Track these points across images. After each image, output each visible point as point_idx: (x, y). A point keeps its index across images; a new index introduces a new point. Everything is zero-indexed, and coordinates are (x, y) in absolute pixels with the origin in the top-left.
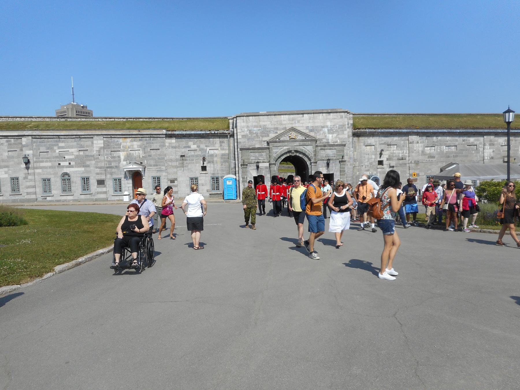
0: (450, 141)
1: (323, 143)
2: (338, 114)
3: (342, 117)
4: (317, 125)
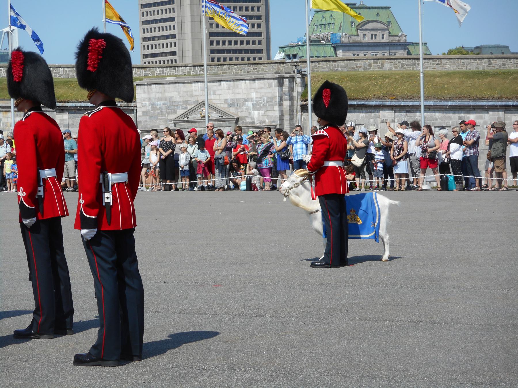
0: (441, 119)
1: (247, 123)
2: (266, 81)
3: (270, 86)
4: (238, 96)
